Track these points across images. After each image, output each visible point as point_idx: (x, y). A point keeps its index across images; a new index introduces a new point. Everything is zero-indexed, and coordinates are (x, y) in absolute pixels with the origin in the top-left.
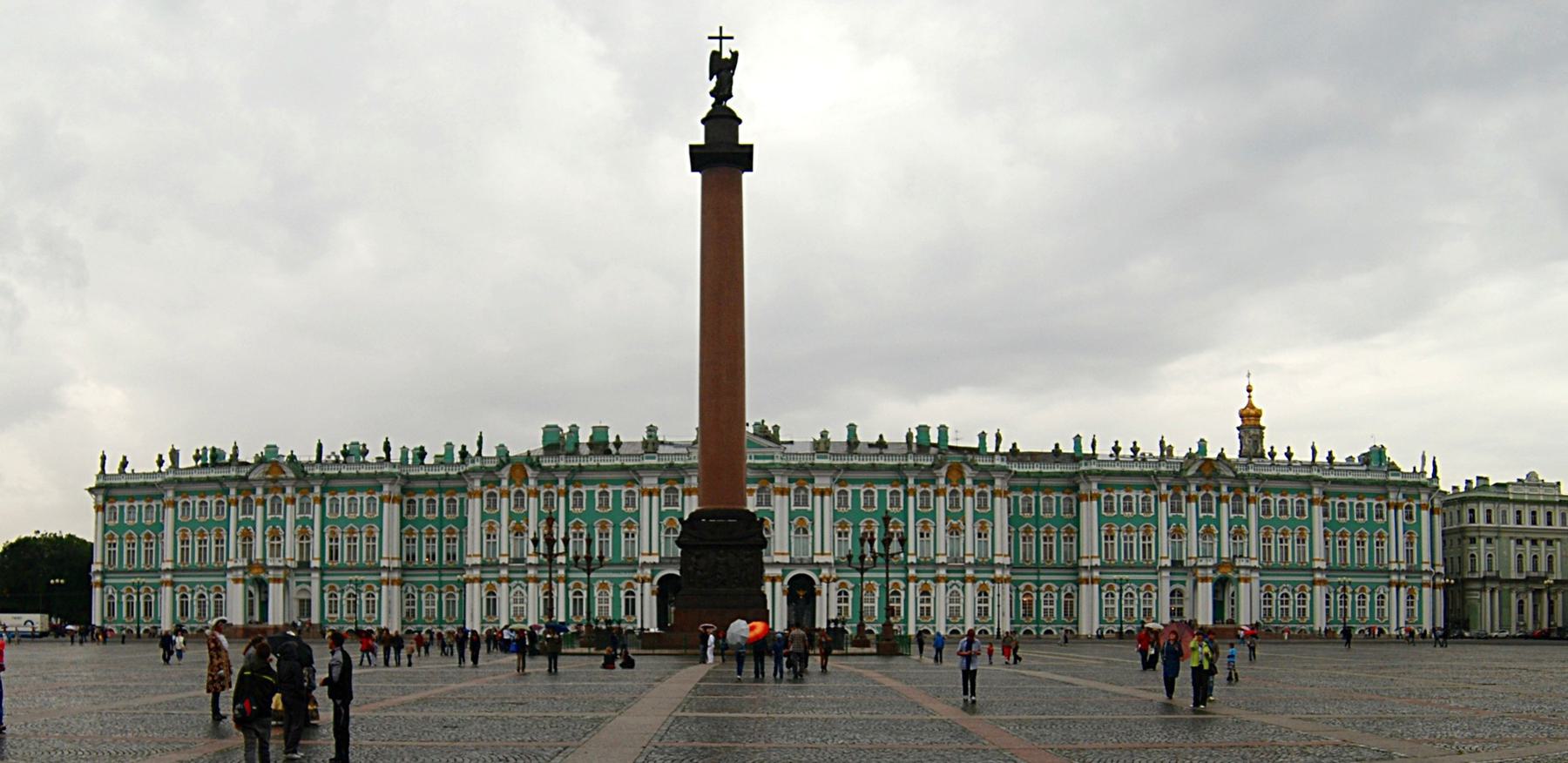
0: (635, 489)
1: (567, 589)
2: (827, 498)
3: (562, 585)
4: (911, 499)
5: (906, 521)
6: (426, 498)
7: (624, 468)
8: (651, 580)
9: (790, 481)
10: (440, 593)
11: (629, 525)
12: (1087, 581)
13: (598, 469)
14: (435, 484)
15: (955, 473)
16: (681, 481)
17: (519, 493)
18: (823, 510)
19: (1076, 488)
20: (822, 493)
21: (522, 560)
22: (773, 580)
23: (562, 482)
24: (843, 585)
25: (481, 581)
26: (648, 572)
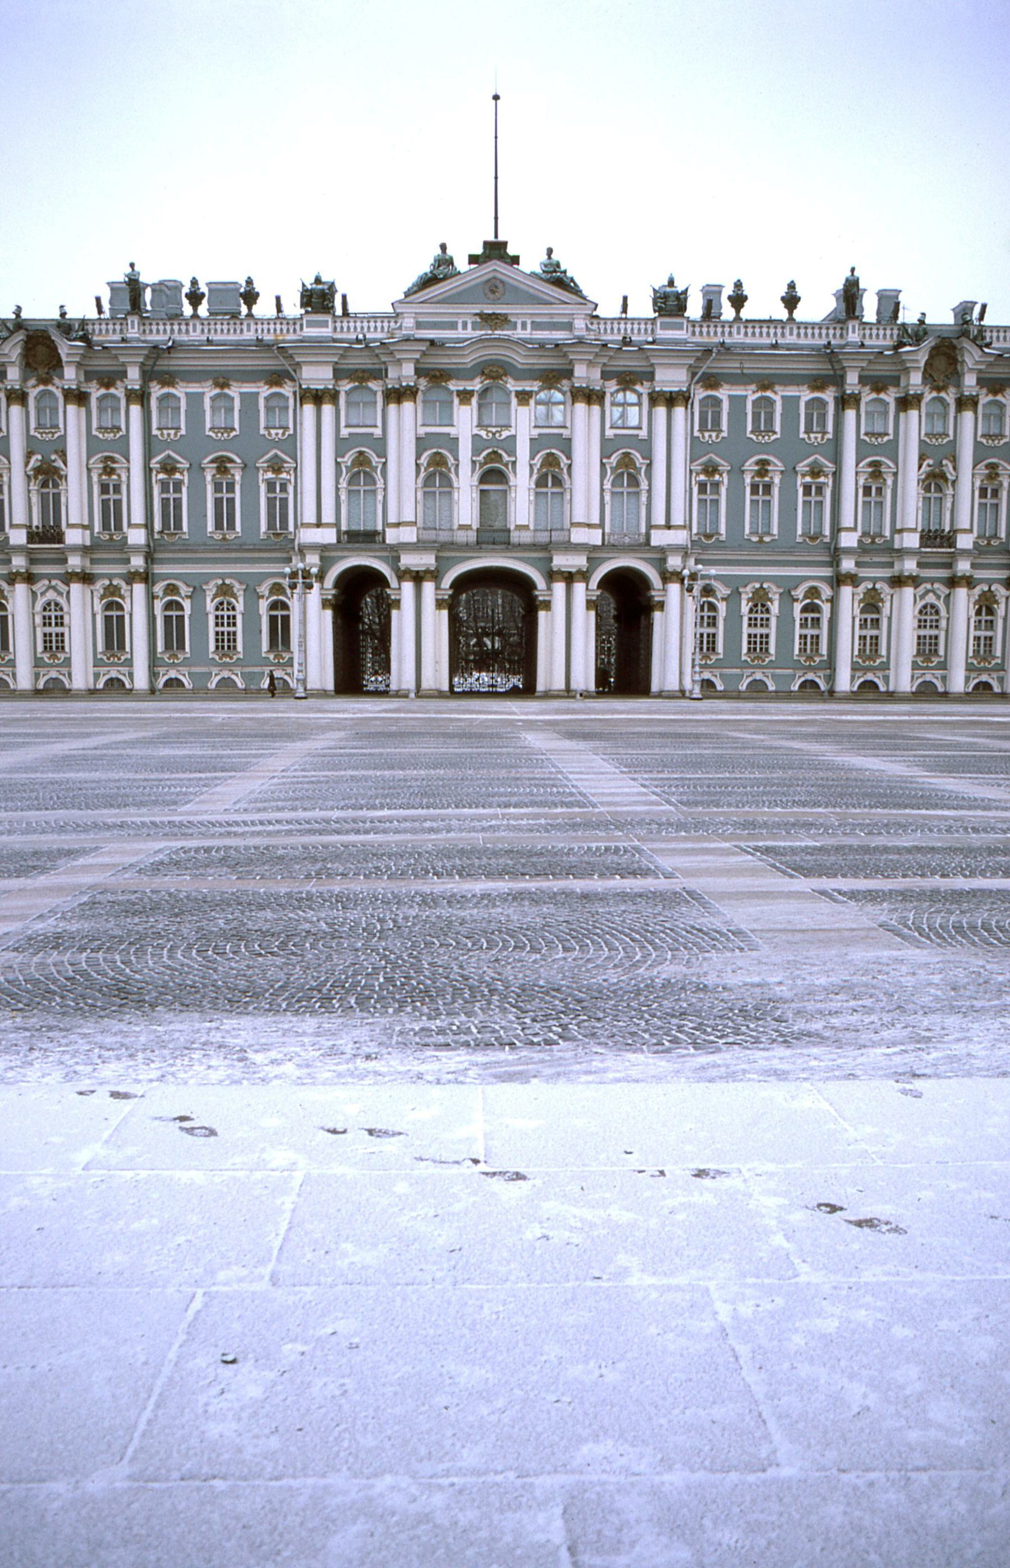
0: (287, 390)
1: (151, 597)
2: (679, 411)
4: (850, 414)
5: (837, 459)
8: (321, 577)
9: (606, 376)
11: (276, 466)
15: (941, 363)
16: (379, 374)
18: (671, 436)
20: (671, 400)
21: (58, 537)
22: (569, 578)
24: (708, 591)
26: (313, 560)
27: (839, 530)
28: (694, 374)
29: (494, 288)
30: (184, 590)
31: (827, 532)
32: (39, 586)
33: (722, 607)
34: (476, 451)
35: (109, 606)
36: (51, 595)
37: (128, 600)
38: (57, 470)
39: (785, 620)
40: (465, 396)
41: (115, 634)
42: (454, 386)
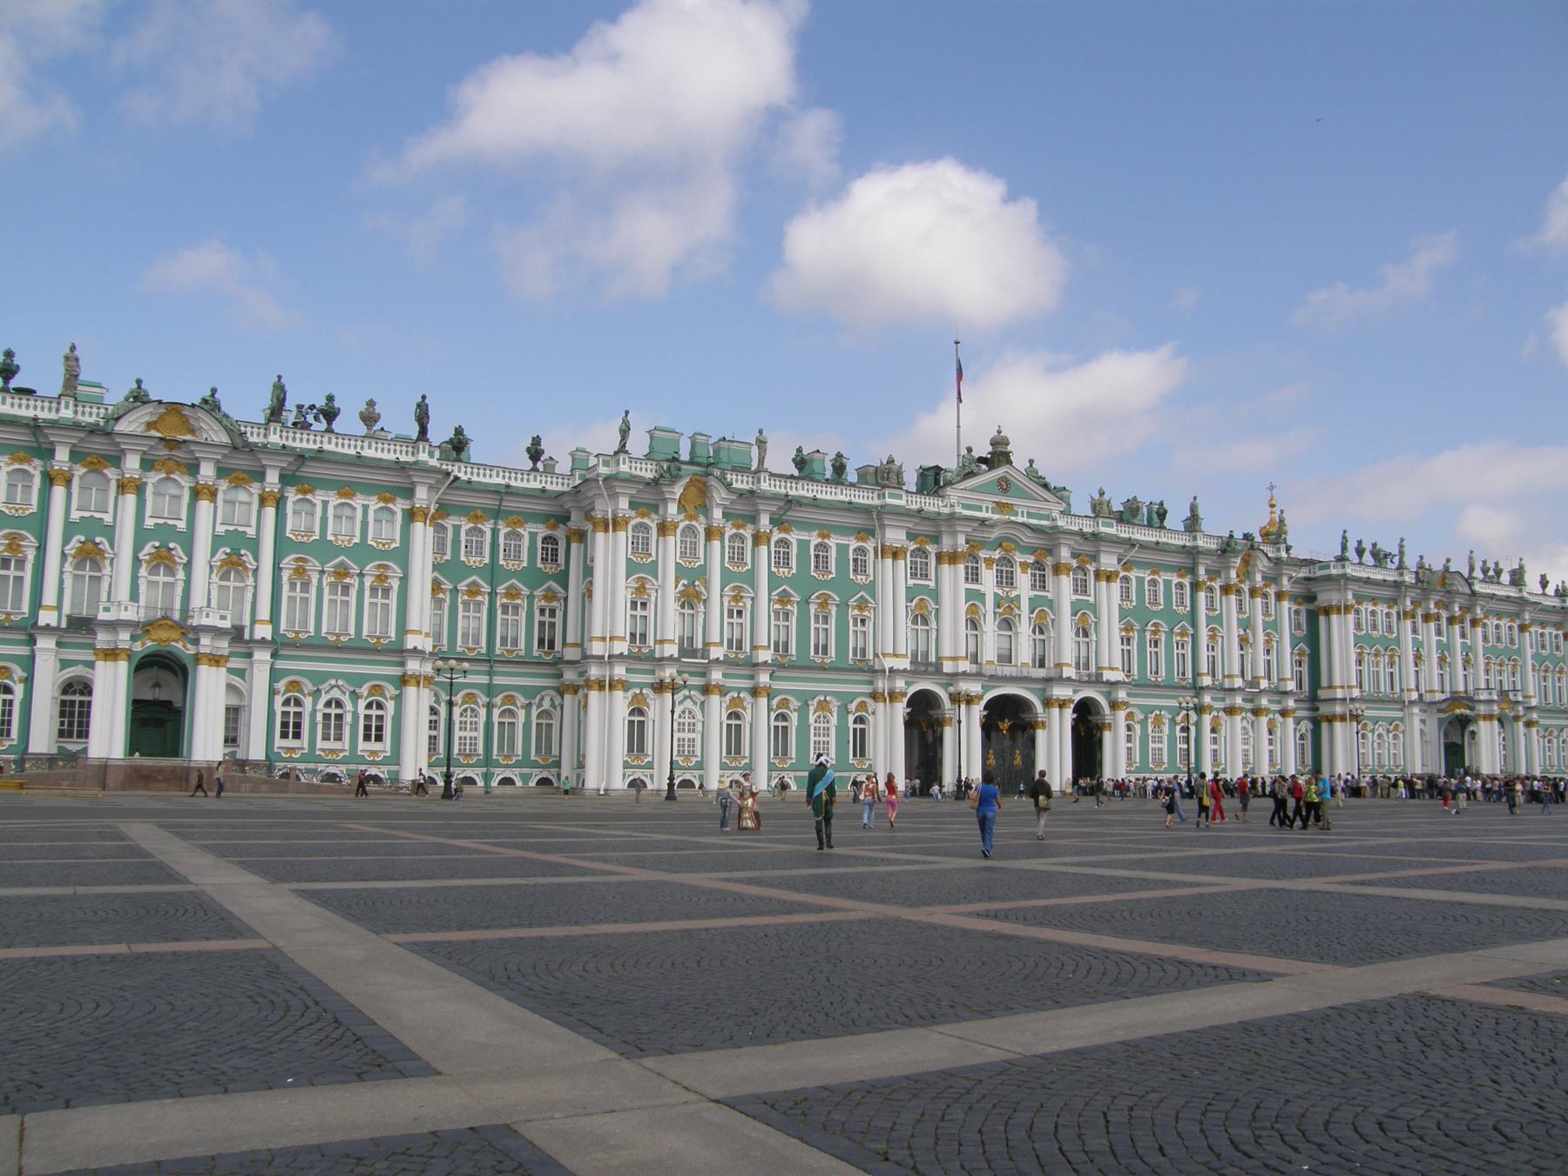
0: (869, 545)
1: (770, 709)
3: (763, 701)
5: (1194, 624)
6: (466, 526)
7: (850, 507)
10: (489, 707)
12: (1343, 718)
13: (815, 503)
14: (490, 502)
16: (936, 539)
17: (690, 530)
19: (1310, 598)
22: (1062, 705)
23: (764, 520)
25: (626, 685)
27: (1200, 675)
28: (1119, 561)
29: (1004, 485)
30: (795, 703)
31: (1189, 675)
32: (679, 697)
33: (1138, 727)
34: (998, 606)
35: (729, 717)
36: (688, 704)
37: (749, 711)
38: (698, 595)
39: (1172, 738)
40: (989, 562)
41: (734, 738)
42: (983, 554)
